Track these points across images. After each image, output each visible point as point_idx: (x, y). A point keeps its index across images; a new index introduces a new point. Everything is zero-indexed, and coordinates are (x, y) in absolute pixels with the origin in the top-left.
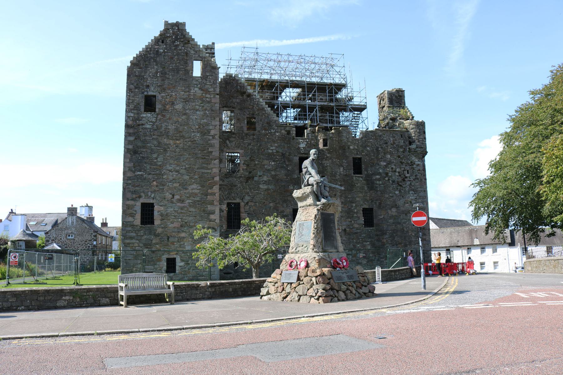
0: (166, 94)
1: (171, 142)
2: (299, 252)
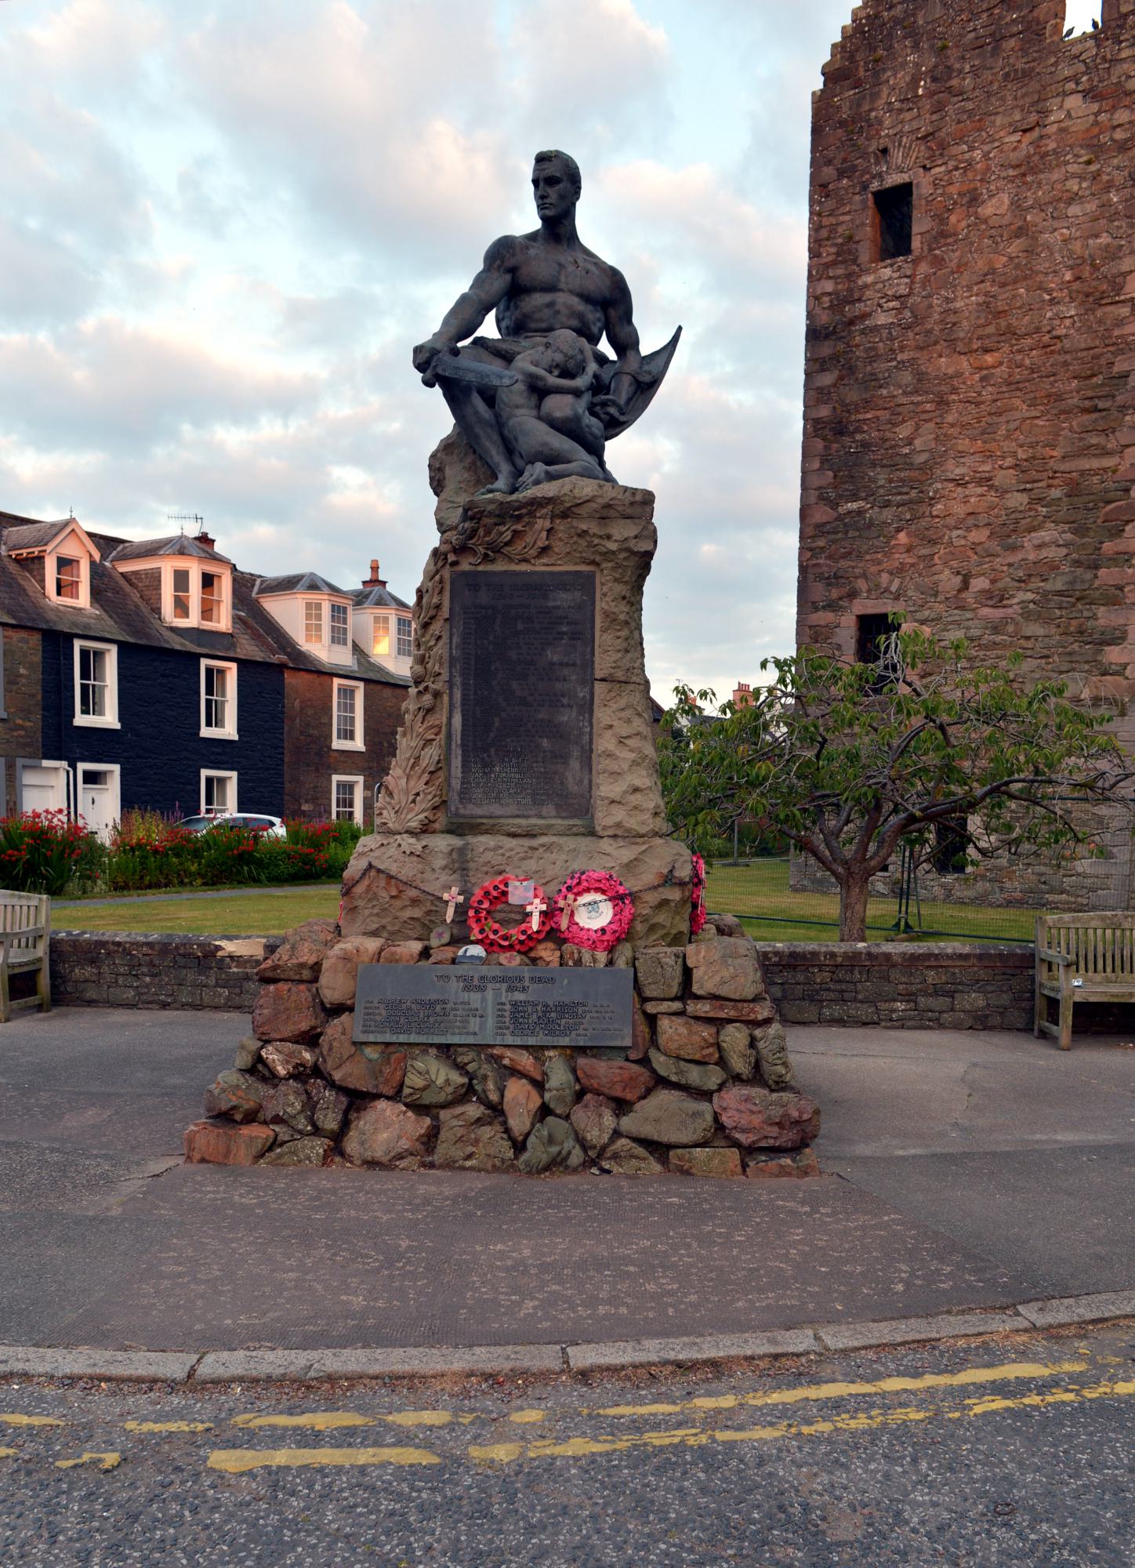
0: (952, 164)
1: (964, 363)
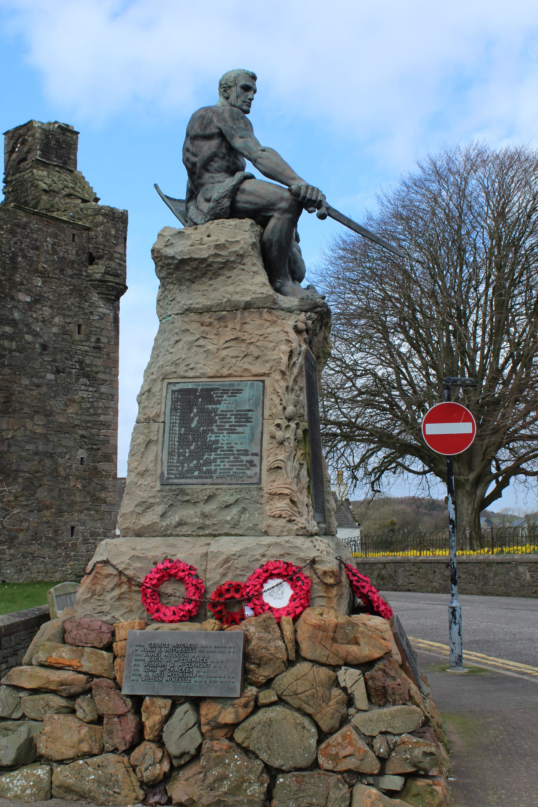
2: (184, 530)
